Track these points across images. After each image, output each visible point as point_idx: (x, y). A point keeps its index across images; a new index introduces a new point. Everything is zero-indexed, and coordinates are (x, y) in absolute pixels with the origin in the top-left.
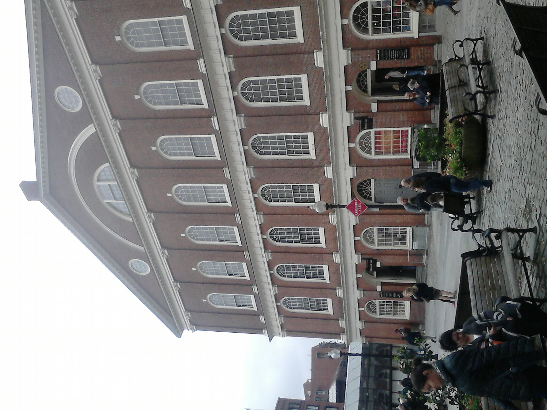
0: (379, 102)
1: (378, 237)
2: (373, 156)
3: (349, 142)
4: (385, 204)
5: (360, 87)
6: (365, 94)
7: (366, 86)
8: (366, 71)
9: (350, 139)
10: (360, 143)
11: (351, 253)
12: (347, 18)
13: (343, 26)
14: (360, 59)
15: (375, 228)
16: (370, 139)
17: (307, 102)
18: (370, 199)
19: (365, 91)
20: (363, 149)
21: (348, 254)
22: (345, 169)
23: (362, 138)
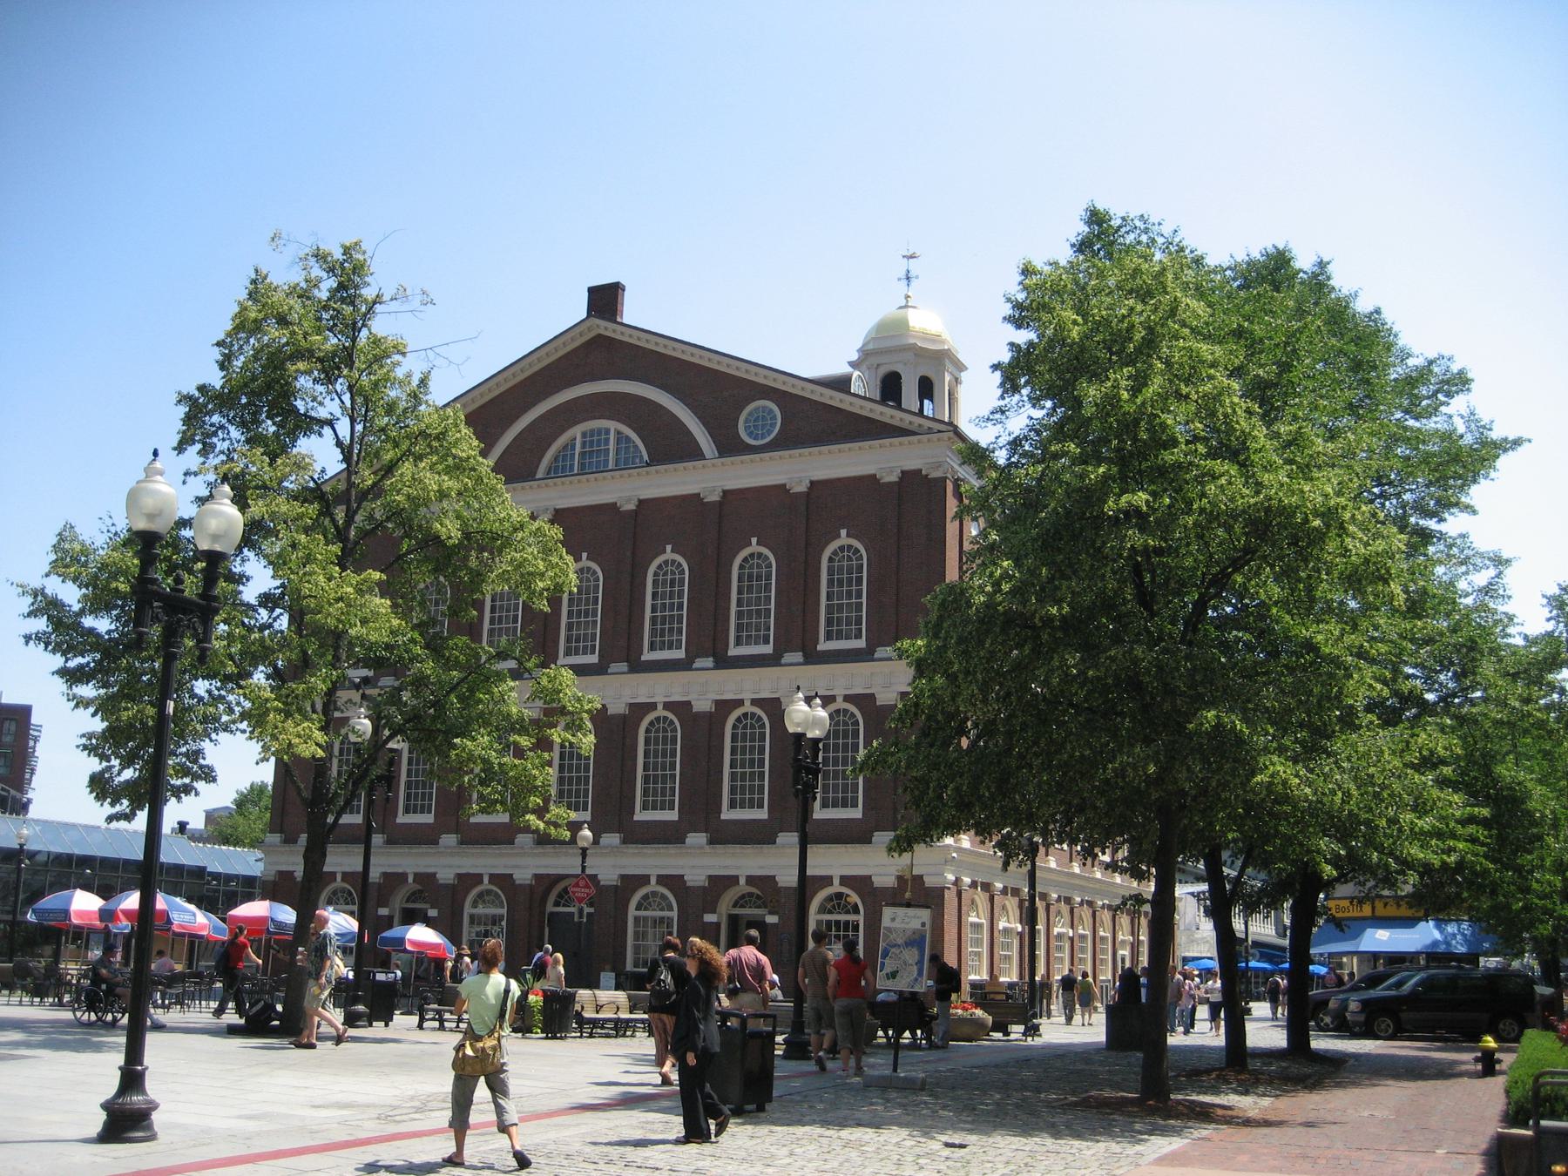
0: (718, 925)
1: (486, 915)
2: (632, 912)
3: (658, 876)
4: (547, 930)
5: (743, 896)
6: (732, 903)
7: (742, 906)
8: (766, 907)
9: (663, 880)
10: (654, 894)
11: (459, 867)
12: (841, 884)
13: (830, 878)
14: (783, 900)
15: (504, 911)
16: (661, 910)
17: (727, 814)
18: (557, 904)
19: (735, 906)
20: (645, 897)
21: (456, 861)
22: (614, 866)
23: (663, 897)
